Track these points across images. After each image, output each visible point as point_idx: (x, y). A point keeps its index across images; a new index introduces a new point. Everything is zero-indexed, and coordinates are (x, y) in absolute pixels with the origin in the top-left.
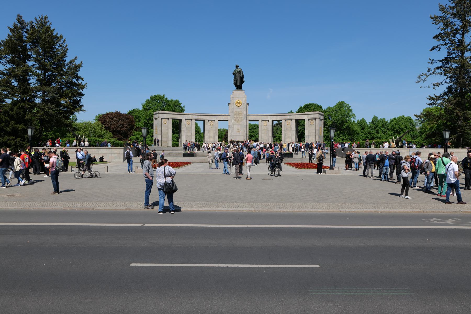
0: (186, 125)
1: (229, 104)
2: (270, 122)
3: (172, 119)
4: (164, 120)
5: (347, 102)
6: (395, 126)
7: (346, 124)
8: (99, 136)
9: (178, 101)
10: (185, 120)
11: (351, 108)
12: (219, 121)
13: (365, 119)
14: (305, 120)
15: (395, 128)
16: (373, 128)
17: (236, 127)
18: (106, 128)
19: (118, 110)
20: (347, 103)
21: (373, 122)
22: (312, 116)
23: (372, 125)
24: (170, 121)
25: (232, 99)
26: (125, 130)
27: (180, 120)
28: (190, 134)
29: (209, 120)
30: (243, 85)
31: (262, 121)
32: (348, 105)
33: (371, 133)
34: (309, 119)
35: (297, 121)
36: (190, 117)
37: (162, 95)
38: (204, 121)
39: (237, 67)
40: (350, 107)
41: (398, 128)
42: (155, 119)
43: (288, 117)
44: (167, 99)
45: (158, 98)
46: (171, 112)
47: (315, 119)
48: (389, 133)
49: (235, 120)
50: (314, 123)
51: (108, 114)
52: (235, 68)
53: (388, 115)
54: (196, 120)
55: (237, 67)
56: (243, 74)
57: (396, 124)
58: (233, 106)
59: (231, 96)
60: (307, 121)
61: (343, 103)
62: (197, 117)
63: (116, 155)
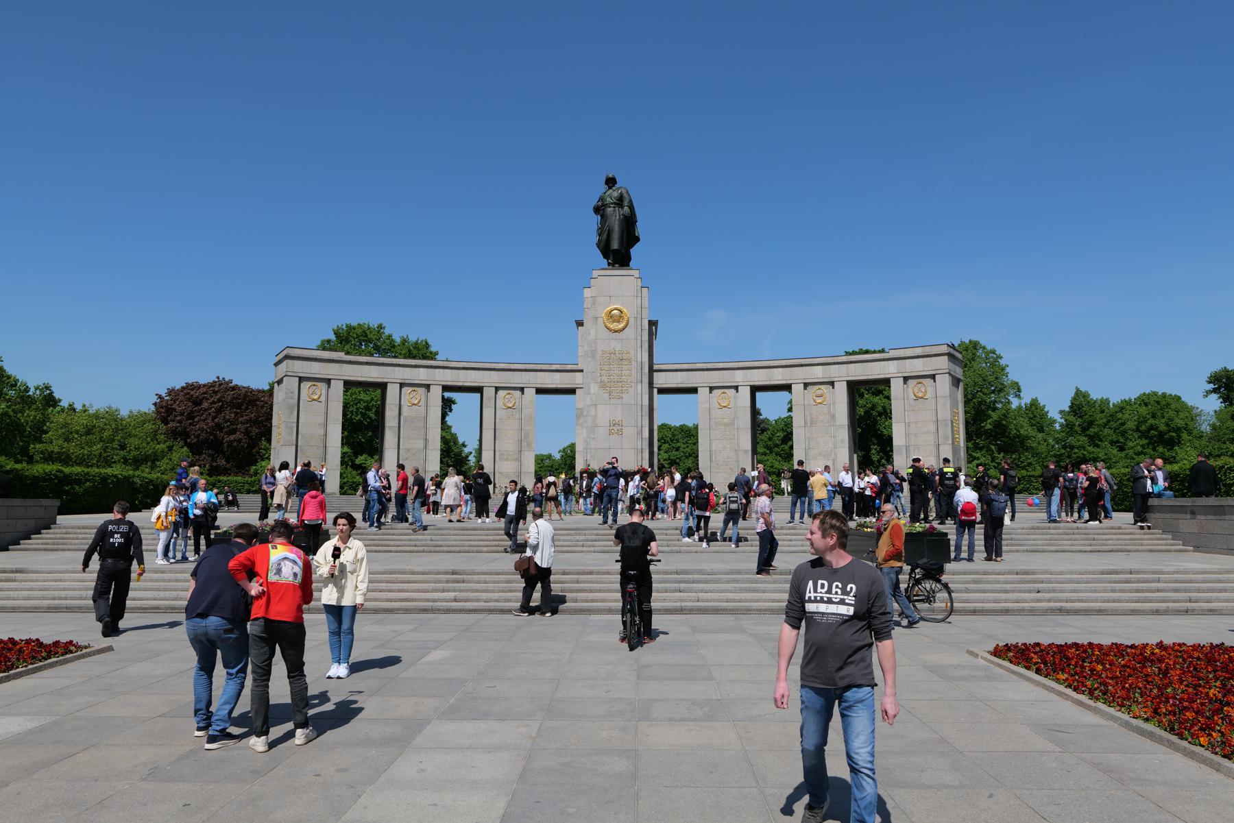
1: (580, 324)
2: (745, 393)
3: (348, 384)
5: (988, 340)
6: (1151, 421)
7: (995, 416)
8: (137, 462)
9: (427, 345)
10: (402, 385)
11: (1002, 362)
12: (540, 391)
13: (1042, 402)
14: (887, 382)
15: (1152, 428)
16: (1077, 429)
17: (605, 414)
18: (174, 434)
20: (989, 348)
22: (918, 367)
23: (1072, 418)
24: (338, 388)
25: (587, 304)
26: (239, 441)
27: (383, 386)
28: (420, 445)
30: (634, 251)
31: (711, 389)
32: (993, 352)
33: (1072, 447)
34: (906, 379)
35: (854, 388)
36: (422, 375)
37: (374, 324)
39: (611, 182)
41: (1163, 428)
43: (818, 373)
46: (340, 355)
47: (933, 377)
48: (1131, 444)
49: (603, 386)
51: (190, 388)
53: (1117, 385)
55: (611, 182)
56: (631, 207)
57: (1154, 416)
58: (593, 332)
60: (896, 388)
61: (975, 345)
62: (450, 377)
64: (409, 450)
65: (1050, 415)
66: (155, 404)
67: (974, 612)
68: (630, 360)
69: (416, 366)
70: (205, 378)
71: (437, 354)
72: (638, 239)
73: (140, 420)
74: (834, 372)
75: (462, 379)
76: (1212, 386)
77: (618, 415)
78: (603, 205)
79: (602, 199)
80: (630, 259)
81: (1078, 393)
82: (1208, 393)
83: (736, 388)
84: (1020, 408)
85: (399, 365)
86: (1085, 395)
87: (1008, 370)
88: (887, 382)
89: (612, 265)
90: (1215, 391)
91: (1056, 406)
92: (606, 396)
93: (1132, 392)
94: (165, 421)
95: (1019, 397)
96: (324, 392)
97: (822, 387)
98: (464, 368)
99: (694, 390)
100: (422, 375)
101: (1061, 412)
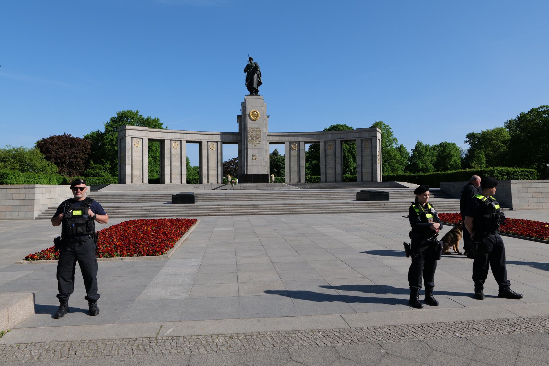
11: (391, 130)
13: (404, 146)
18: (48, 159)
19: (68, 132)
20: (386, 124)
22: (366, 135)
24: (146, 143)
27: (162, 142)
30: (259, 89)
32: (388, 126)
36: (178, 137)
37: (134, 111)
38: (200, 143)
39: (250, 59)
40: (390, 128)
42: (120, 139)
44: (141, 116)
46: (146, 128)
50: (370, 146)
51: (51, 138)
52: (247, 63)
54: (188, 142)
55: (250, 59)
60: (358, 143)
63: (16, 203)
65: (407, 151)
67: (398, 212)
71: (162, 124)
72: (261, 83)
73: (32, 152)
76: (467, 139)
77: (256, 154)
80: (258, 91)
82: (466, 142)
84: (397, 148)
86: (421, 144)
87: (393, 133)
89: (251, 94)
90: (468, 141)
91: (409, 148)
99: (283, 143)
101: (412, 150)
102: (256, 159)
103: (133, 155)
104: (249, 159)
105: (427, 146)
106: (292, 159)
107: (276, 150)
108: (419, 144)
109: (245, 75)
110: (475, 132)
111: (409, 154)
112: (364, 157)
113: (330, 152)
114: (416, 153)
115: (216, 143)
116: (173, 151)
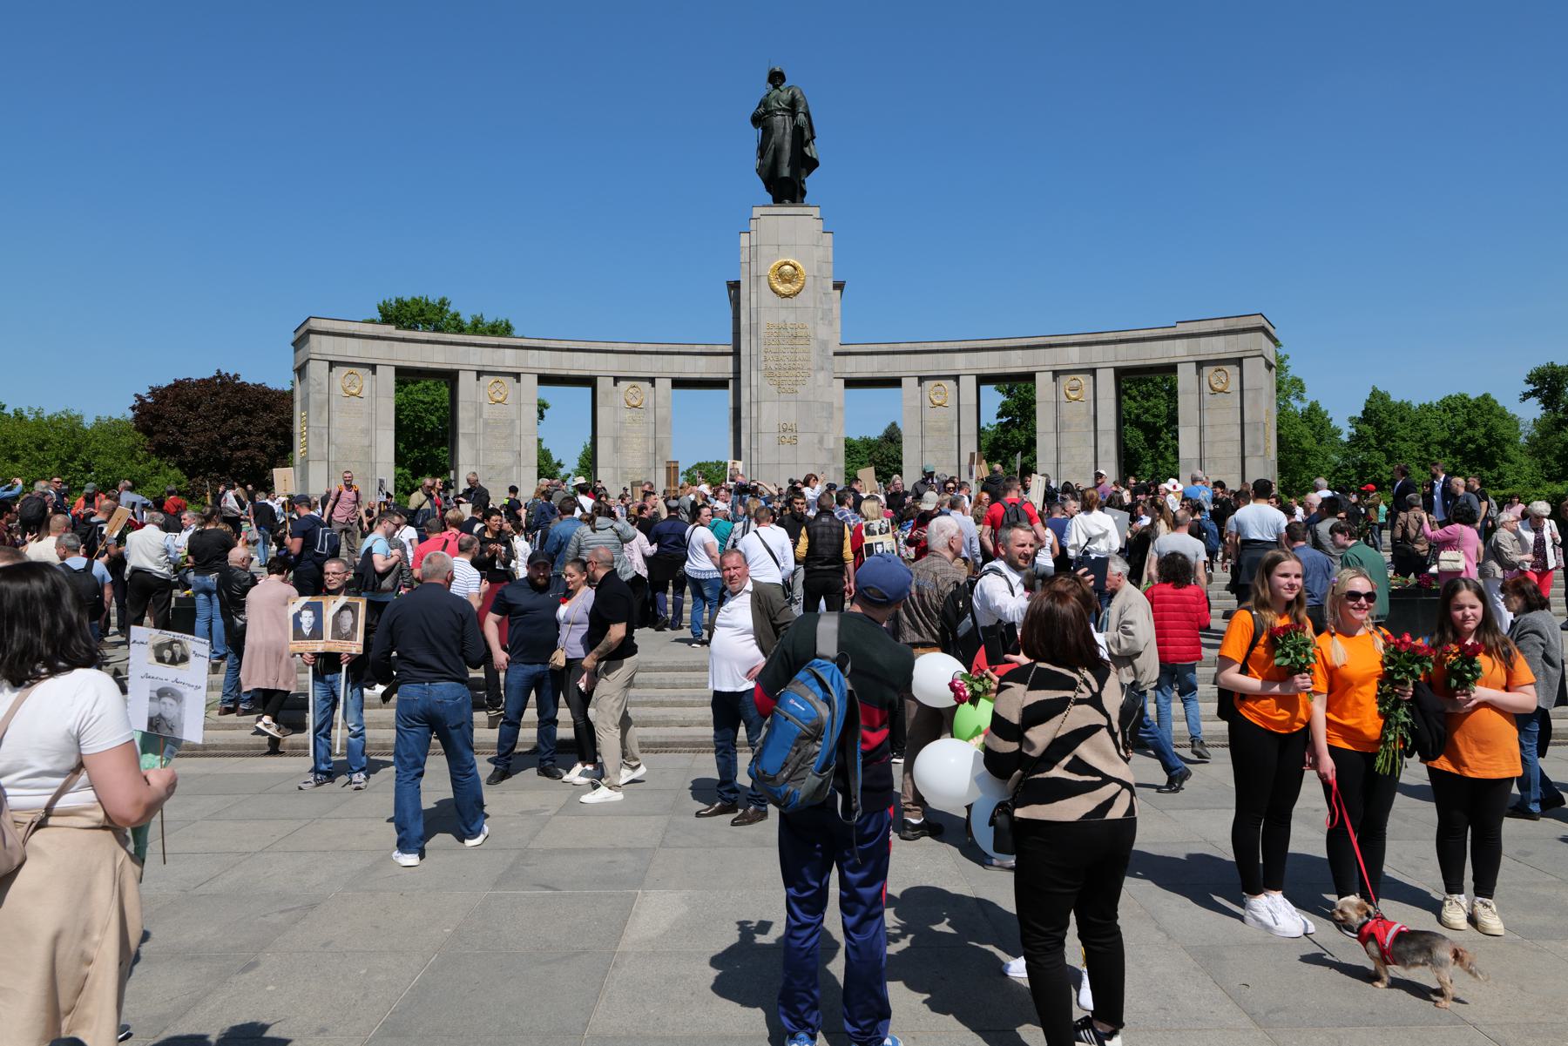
0: (486, 408)
2: (968, 384)
4: (346, 370)
6: (1469, 432)
10: (480, 374)
12: (678, 383)
14: (1172, 368)
15: (1471, 440)
18: (161, 450)
19: (230, 370)
21: (1369, 416)
24: (387, 377)
27: (450, 377)
29: (617, 380)
30: (811, 182)
31: (921, 379)
35: (1126, 377)
36: (508, 359)
37: (434, 298)
39: (776, 78)
41: (1483, 442)
45: (415, 310)
46: (390, 330)
49: (770, 375)
50: (1234, 385)
51: (179, 385)
52: (763, 88)
53: (1420, 384)
54: (544, 380)
55: (776, 78)
56: (807, 115)
59: (744, 237)
60: (1186, 379)
64: (492, 468)
65: (1333, 424)
66: (133, 408)
68: (807, 337)
69: (499, 346)
70: (200, 370)
73: (110, 430)
74: (1096, 355)
75: (566, 365)
76: (1531, 387)
78: (767, 112)
79: (764, 103)
80: (803, 193)
81: (1375, 393)
82: (1526, 396)
83: (956, 378)
85: (475, 345)
86: (1384, 397)
88: (1172, 368)
89: (778, 200)
90: (1534, 393)
91: (1343, 414)
92: (774, 389)
93: (1435, 397)
94: (148, 432)
95: (1299, 398)
96: (366, 383)
97: (1079, 377)
98: (569, 350)
99: (895, 382)
100: (508, 359)
101: (1351, 419)
102: (794, 442)
103: (337, 421)
104: (767, 441)
105: (1402, 407)
106: (928, 441)
107: (894, 424)
108: (1377, 397)
109: (755, 134)
110: (1558, 363)
111: (1339, 432)
112: (1207, 430)
113: (1078, 413)
114: (1368, 429)
115: (648, 385)
116: (487, 411)
